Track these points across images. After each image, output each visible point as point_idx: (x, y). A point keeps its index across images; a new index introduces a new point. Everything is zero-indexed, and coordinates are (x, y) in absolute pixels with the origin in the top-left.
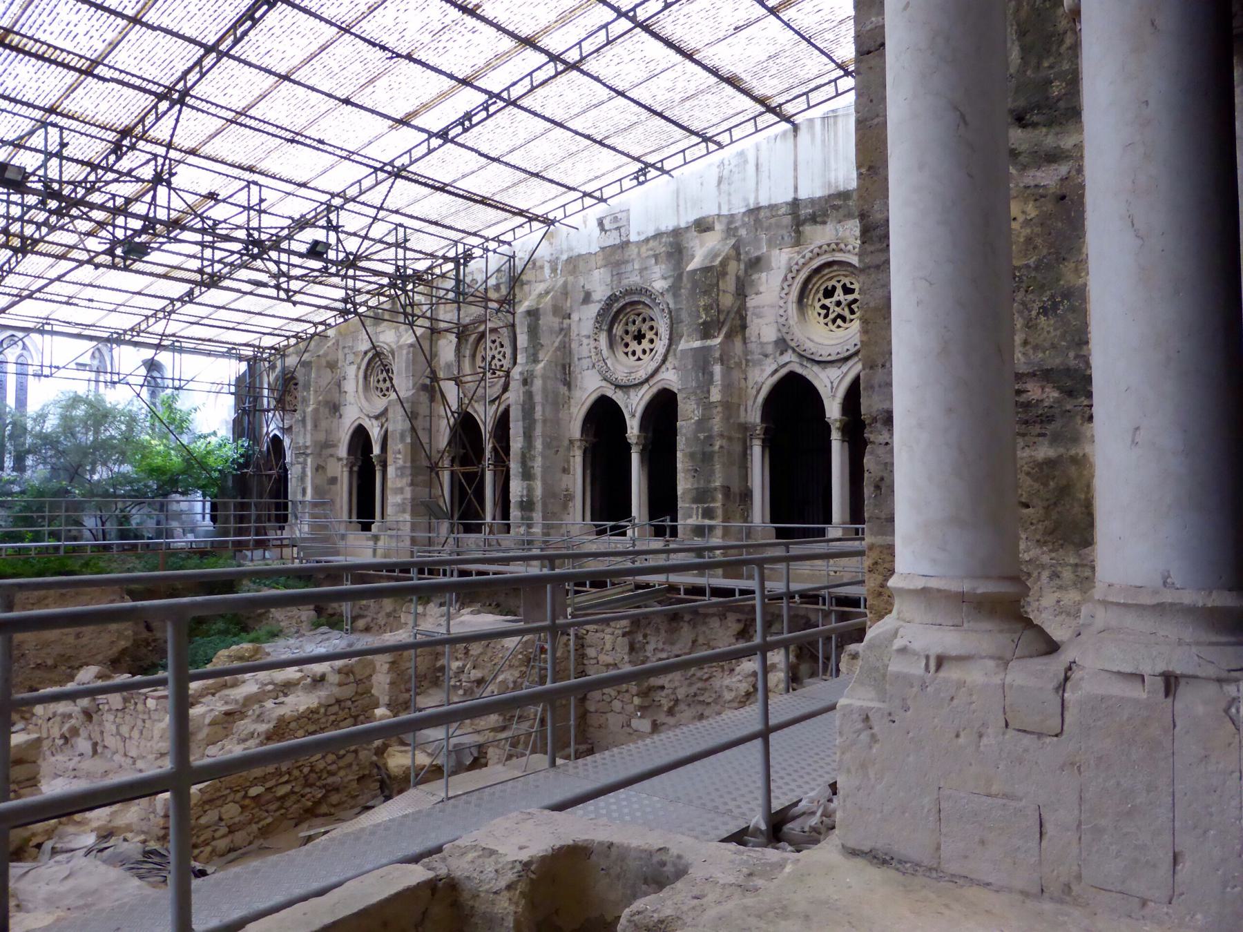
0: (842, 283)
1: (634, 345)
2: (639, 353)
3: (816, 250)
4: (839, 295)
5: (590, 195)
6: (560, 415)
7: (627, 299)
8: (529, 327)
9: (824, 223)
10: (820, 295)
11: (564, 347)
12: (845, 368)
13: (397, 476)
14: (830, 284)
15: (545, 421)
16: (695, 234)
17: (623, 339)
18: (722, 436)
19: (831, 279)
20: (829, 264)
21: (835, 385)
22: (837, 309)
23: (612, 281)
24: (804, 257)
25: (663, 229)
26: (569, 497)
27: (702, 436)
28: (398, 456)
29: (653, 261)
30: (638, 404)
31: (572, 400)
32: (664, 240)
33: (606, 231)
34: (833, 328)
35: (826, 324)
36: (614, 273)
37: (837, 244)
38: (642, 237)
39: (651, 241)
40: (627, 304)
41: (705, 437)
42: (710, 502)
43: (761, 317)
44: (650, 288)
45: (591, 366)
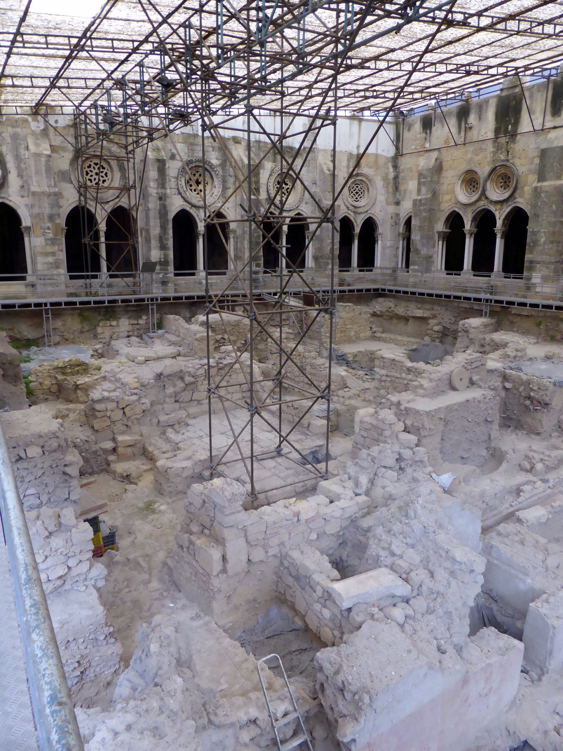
8: (158, 168)
13: (47, 244)
28: (47, 231)
29: (211, 149)
45: (177, 192)
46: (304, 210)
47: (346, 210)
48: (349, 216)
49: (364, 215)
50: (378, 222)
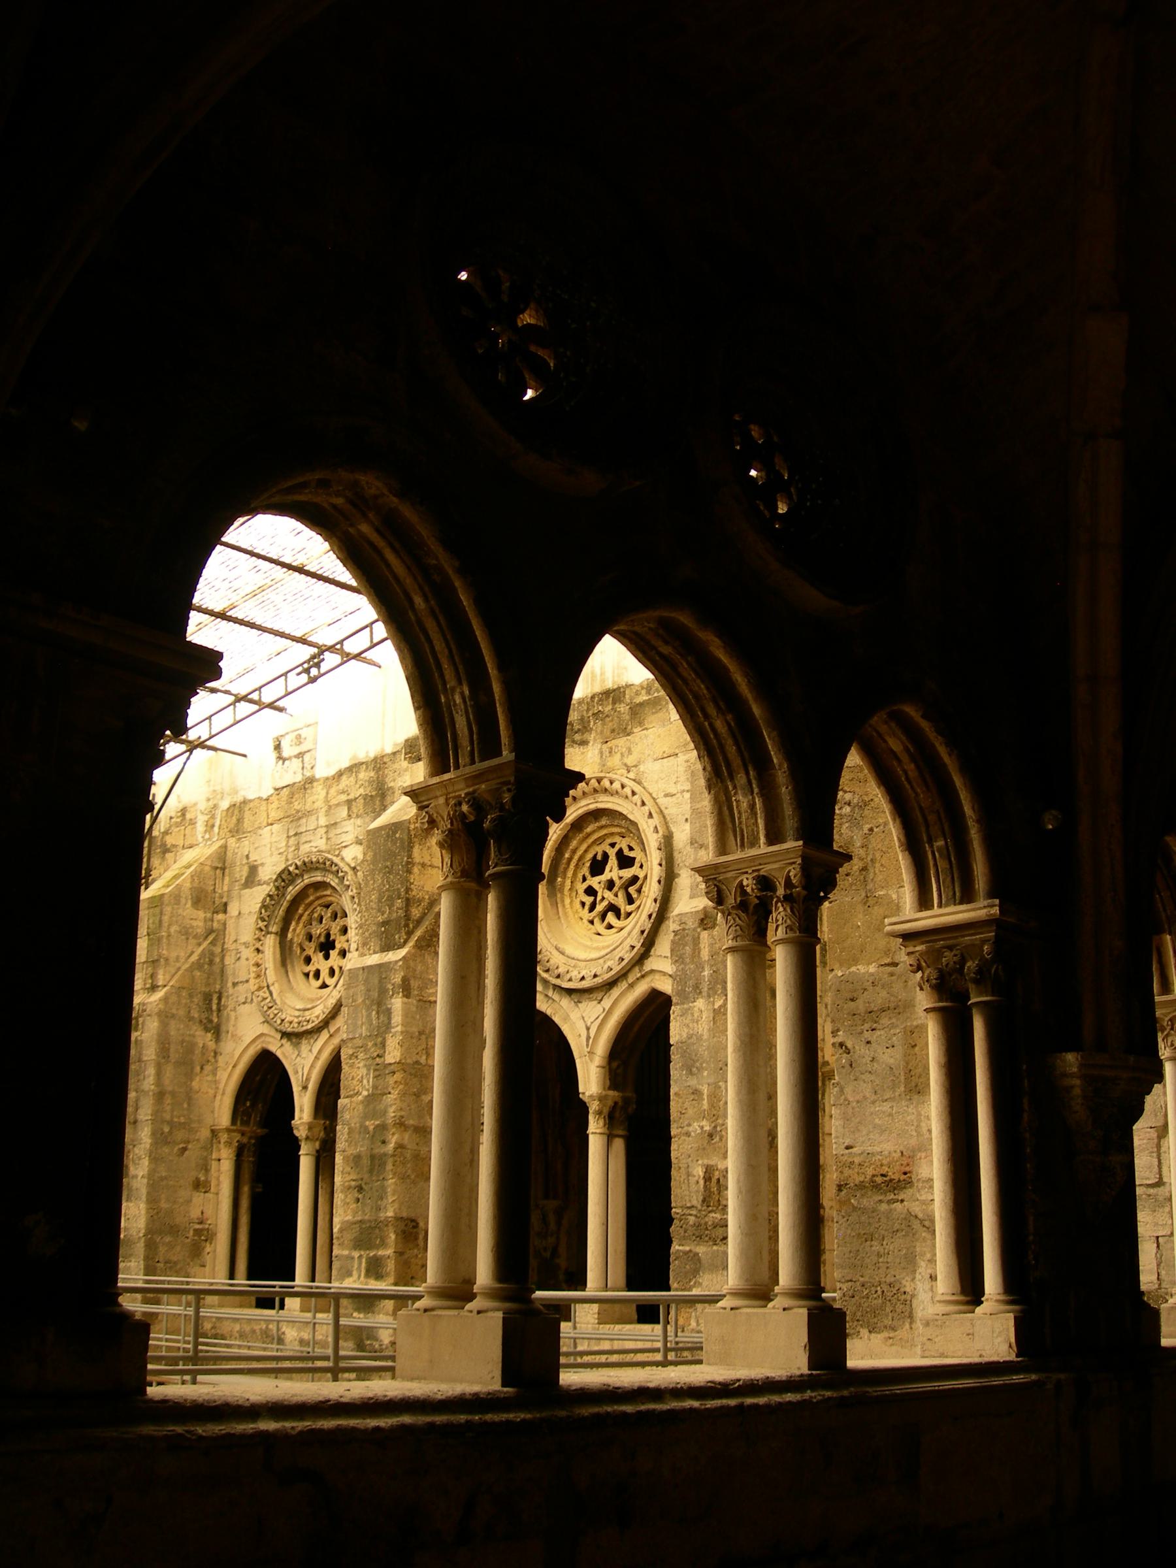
1: (319, 961)
2: (324, 974)
5: (244, 698)
6: (195, 1084)
7: (307, 879)
9: (584, 743)
10: (585, 870)
11: (211, 963)
12: (607, 1003)
14: (599, 850)
15: (160, 1096)
16: (405, 764)
17: (303, 950)
18: (401, 1124)
21: (592, 1033)
23: (287, 846)
25: (362, 757)
26: (205, 1235)
27: (370, 1124)
29: (344, 812)
30: (312, 1066)
31: (220, 1059)
32: (363, 775)
33: (284, 760)
34: (599, 926)
35: (592, 922)
36: (292, 833)
37: (599, 781)
38: (332, 771)
39: (344, 777)
40: (308, 887)
41: (377, 1127)
42: (378, 1248)
44: (336, 860)
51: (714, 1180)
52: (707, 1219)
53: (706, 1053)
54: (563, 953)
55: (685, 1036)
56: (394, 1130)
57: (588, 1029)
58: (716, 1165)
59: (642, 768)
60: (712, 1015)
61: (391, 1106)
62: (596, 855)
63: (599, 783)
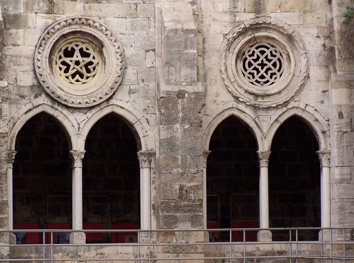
0: (79, 47)
3: (70, 21)
4: (77, 56)
10: (62, 53)
12: (89, 114)
19: (71, 43)
20: (74, 33)
22: (76, 66)
24: (59, 24)
34: (73, 81)
35: (67, 77)
43: (18, 65)
46: (127, 106)
47: (235, 104)
48: (242, 116)
49: (280, 112)
50: (317, 128)
51: (184, 191)
52: (180, 204)
53: (180, 144)
54: (63, 91)
55: (169, 137)
56: (5, 163)
57: (79, 124)
58: (186, 185)
59: (107, 19)
60: (183, 131)
61: (3, 152)
62: (68, 48)
63: (94, 23)
